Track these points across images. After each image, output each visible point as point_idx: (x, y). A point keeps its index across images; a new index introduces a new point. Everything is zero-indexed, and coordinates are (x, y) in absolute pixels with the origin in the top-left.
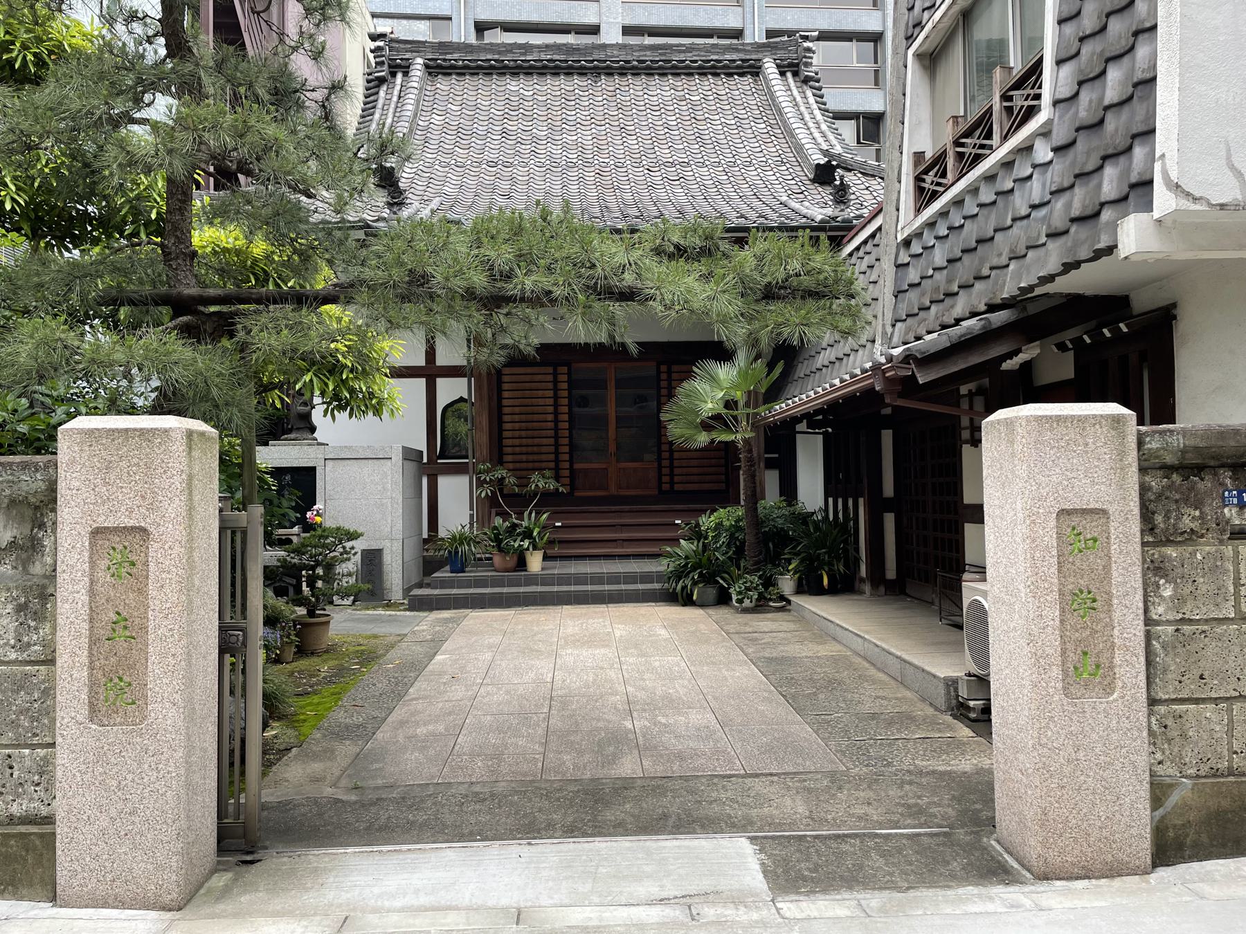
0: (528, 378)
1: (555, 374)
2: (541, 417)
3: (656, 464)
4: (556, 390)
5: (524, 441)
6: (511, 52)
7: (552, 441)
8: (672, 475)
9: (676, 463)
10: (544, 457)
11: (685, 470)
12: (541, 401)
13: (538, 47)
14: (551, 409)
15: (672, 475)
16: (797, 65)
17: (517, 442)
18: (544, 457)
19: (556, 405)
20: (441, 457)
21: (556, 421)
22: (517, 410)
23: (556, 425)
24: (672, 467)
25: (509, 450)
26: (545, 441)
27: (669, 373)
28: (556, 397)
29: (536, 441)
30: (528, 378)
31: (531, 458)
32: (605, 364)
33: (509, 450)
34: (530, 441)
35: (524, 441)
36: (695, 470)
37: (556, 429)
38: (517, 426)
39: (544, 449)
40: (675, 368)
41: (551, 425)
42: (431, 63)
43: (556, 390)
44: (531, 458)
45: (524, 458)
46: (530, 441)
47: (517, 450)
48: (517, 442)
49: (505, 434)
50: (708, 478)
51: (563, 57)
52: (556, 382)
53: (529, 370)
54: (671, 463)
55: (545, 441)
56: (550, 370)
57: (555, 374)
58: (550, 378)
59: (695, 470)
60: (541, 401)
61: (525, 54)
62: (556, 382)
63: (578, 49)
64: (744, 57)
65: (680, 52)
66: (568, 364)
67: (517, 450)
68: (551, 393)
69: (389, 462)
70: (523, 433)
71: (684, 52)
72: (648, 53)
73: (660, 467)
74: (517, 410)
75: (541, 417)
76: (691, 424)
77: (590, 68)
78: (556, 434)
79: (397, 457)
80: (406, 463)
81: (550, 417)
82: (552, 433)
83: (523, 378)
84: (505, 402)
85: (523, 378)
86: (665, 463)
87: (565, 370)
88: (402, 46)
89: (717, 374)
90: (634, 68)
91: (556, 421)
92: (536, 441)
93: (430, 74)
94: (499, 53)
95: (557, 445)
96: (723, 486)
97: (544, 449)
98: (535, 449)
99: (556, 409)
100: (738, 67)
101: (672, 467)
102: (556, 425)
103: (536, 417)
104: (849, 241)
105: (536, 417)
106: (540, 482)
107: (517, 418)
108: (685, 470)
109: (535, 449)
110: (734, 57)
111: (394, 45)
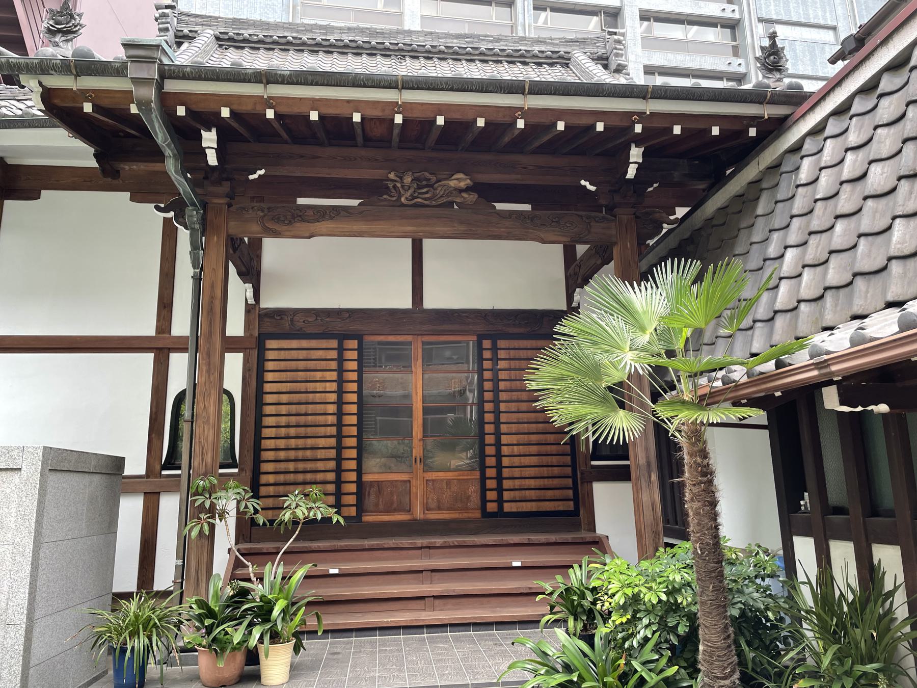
0: (302, 354)
1: (341, 349)
2: (319, 408)
3: (477, 475)
4: (341, 370)
5: (293, 443)
6: (311, 31)
7: (333, 442)
8: (500, 490)
9: (506, 472)
10: (320, 465)
11: (517, 483)
12: (319, 387)
13: (340, 29)
14: (333, 397)
15: (500, 490)
16: (607, 59)
17: (282, 443)
18: (320, 465)
19: (340, 392)
20: (166, 467)
21: (340, 414)
22: (284, 398)
23: (340, 420)
24: (499, 478)
25: (269, 455)
26: (322, 442)
27: (495, 349)
28: (340, 381)
29: (310, 442)
30: (302, 354)
31: (301, 466)
32: (409, 338)
33: (269, 455)
34: (300, 443)
35: (293, 443)
36: (532, 483)
37: (340, 425)
38: (283, 420)
39: (320, 454)
40: (502, 343)
41: (332, 419)
42: (222, 36)
43: (341, 370)
44: (301, 466)
45: (291, 466)
46: (300, 443)
47: (282, 455)
48: (282, 443)
49: (266, 432)
50: (549, 494)
51: (366, 39)
52: (341, 360)
53: (304, 343)
54: (499, 473)
55: (322, 442)
56: (334, 343)
57: (341, 349)
58: (334, 354)
59: (532, 483)
60: (319, 387)
61: (325, 34)
62: (341, 360)
63: (382, 33)
64: (553, 49)
65: (488, 41)
66: (359, 337)
67: (282, 455)
68: (333, 376)
69: (15, 478)
70: (292, 431)
71: (491, 41)
72: (455, 41)
73: (483, 479)
74: (284, 398)
75: (319, 408)
76: (589, 396)
77: (395, 51)
78: (339, 431)
79: (32, 469)
80: (53, 478)
81: (332, 408)
82: (333, 430)
83: (294, 355)
84: (268, 387)
85: (294, 355)
86: (491, 473)
87: (354, 344)
88: (191, 19)
89: (630, 302)
90: (440, 52)
91: (340, 414)
92: (310, 442)
93: (220, 46)
94: (298, 32)
95: (339, 448)
96: (570, 506)
97: (320, 454)
98: (309, 454)
99: (340, 397)
100: (547, 57)
101: (499, 478)
102: (340, 420)
103: (310, 408)
104: (885, 42)
105: (310, 408)
107: (284, 409)
108: (517, 483)
109: (309, 454)
110: (543, 49)
111: (183, 18)
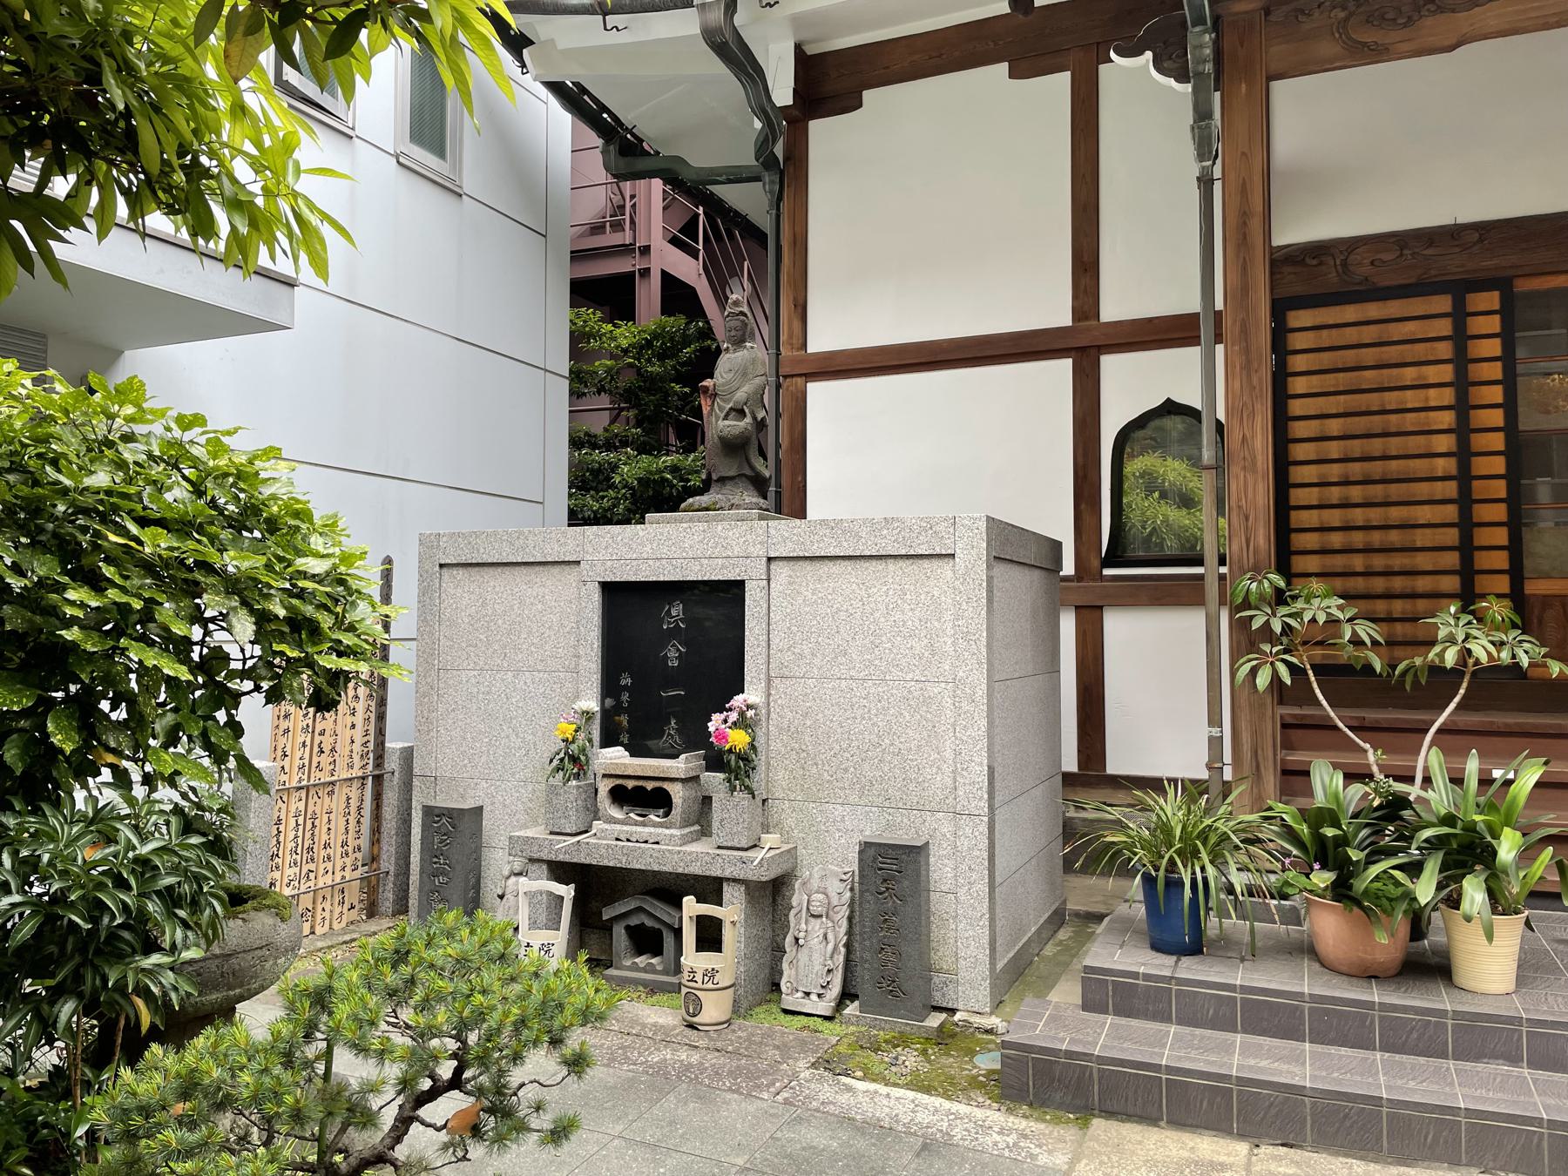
1: (1460, 315)
2: (1415, 444)
4: (1461, 360)
7: (1451, 512)
14: (1447, 419)
17: (1334, 517)
18: (1423, 561)
19: (1463, 407)
20: (1110, 561)
26: (1424, 514)
29: (1396, 514)
30: (1369, 334)
31: (1379, 562)
37: (1465, 477)
38: (1334, 472)
43: (1461, 360)
44: (1379, 562)
46: (1375, 516)
47: (1336, 540)
48: (1334, 517)
52: (1461, 338)
53: (1373, 310)
55: (1424, 514)
56: (1443, 303)
57: (1460, 315)
58: (1444, 327)
62: (1461, 338)
66: (1502, 284)
67: (1336, 540)
69: (945, 568)
74: (1334, 427)
75: (1415, 444)
79: (972, 551)
80: (1000, 569)
83: (1351, 335)
85: (1351, 335)
87: (1491, 299)
91: (1464, 454)
92: (1396, 514)
95: (1467, 525)
97: (1422, 538)
98: (1394, 537)
103: (1395, 445)
105: (1395, 445)
106: (1468, 639)
107: (1334, 449)
109: (1394, 537)
